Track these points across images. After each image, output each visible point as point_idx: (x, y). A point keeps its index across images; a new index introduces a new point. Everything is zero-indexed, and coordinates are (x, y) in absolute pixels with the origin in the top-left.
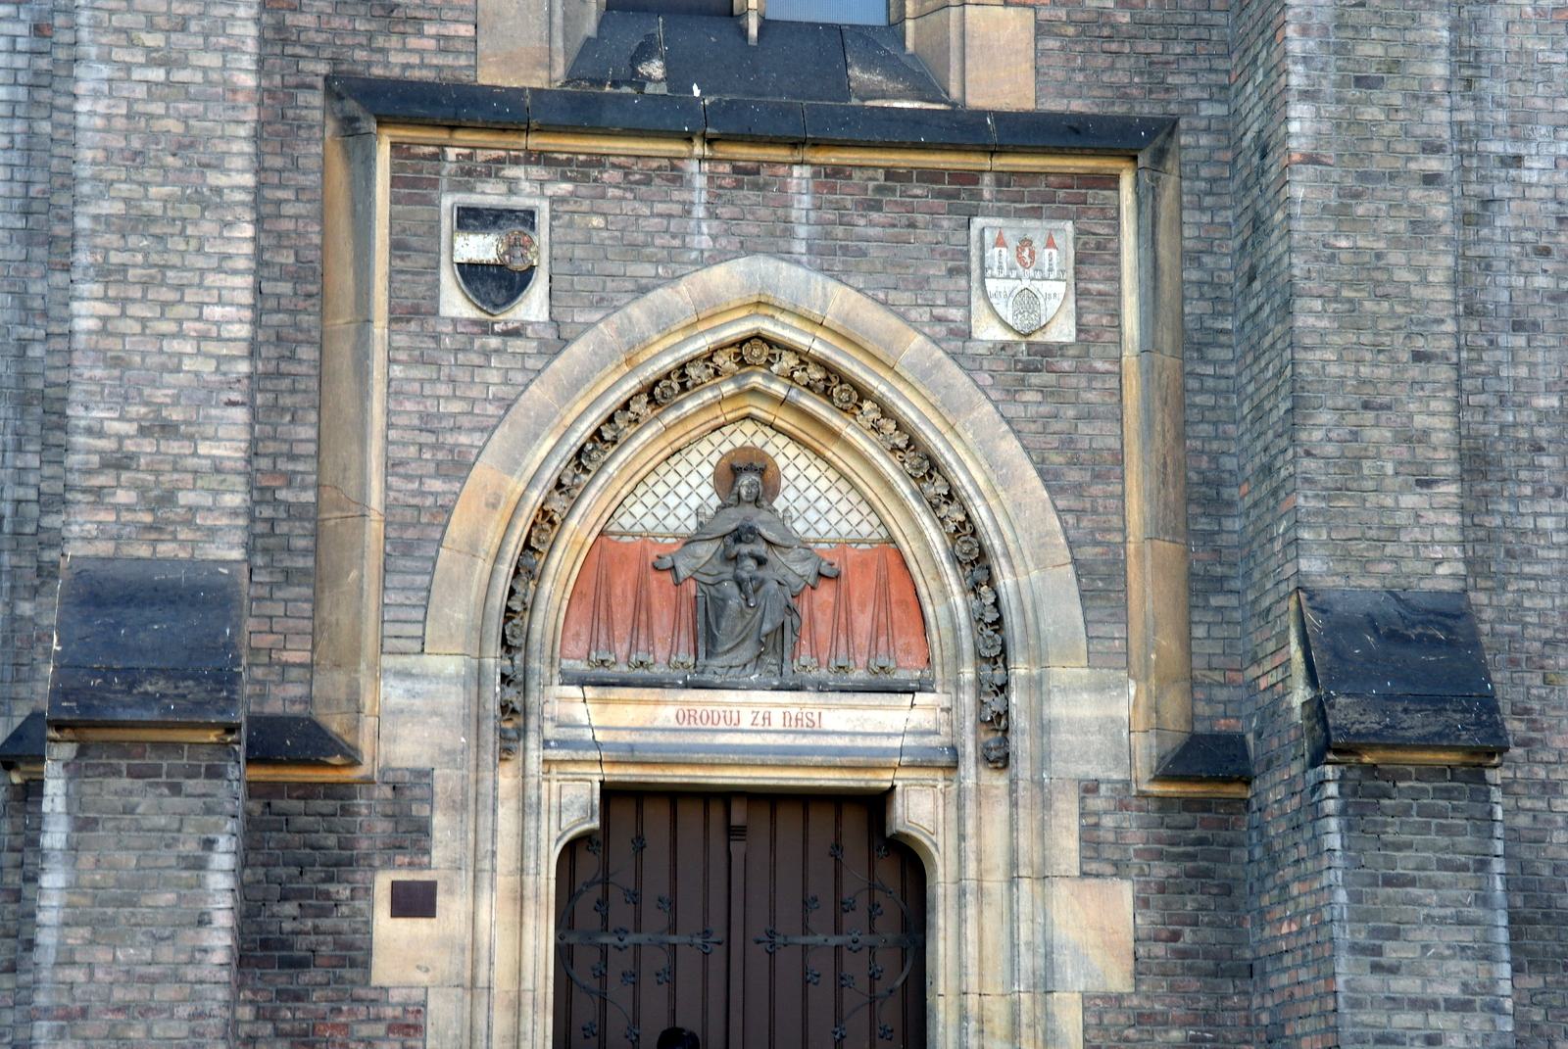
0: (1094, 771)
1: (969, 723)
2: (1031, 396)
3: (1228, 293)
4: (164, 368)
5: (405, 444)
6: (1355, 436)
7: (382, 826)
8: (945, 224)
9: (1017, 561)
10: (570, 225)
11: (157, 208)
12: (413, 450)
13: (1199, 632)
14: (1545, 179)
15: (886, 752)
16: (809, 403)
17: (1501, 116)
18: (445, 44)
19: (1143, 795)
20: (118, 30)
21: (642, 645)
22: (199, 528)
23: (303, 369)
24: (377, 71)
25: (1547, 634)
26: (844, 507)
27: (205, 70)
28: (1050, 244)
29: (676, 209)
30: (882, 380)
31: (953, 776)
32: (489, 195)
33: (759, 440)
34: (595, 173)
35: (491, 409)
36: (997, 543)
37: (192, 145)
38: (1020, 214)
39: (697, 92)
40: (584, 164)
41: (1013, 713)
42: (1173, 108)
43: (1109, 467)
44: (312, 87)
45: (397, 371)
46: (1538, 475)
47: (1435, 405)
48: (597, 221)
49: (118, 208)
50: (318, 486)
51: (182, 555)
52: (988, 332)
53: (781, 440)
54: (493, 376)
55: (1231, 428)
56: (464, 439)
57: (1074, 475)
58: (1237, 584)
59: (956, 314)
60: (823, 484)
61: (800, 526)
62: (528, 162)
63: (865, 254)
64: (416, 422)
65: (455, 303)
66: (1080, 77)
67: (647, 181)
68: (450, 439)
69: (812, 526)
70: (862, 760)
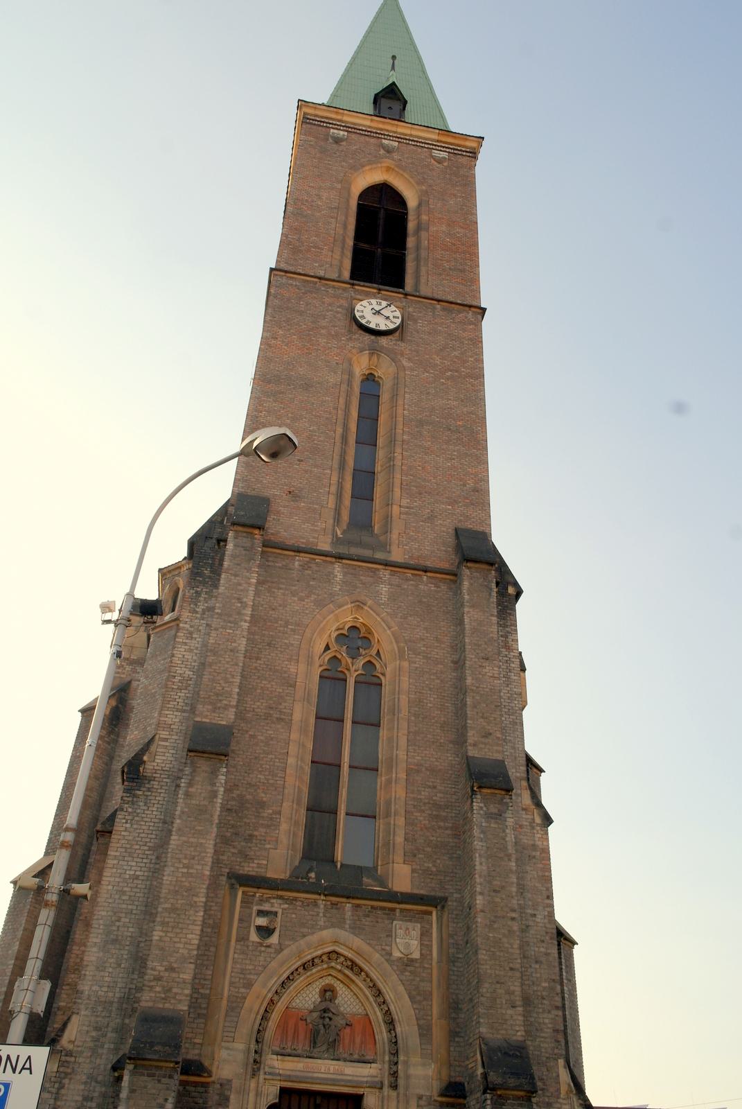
0: (421, 1092)
1: (387, 1074)
2: (407, 973)
3: (460, 947)
4: (174, 951)
5: (236, 977)
6: (495, 991)
7: (216, 1097)
8: (386, 922)
9: (402, 1023)
10: (287, 916)
11: (179, 906)
12: (237, 979)
13: (452, 1049)
14: (542, 921)
15: (362, 1082)
16: (347, 972)
17: (530, 903)
18: (259, 866)
19: (435, 1101)
20: (177, 858)
21: (295, 1043)
22: (177, 1000)
23: (211, 954)
24: (241, 872)
25: (547, 1055)
26: (354, 1004)
27: (197, 869)
28: (414, 930)
29: (315, 914)
30: (366, 965)
31: (381, 1091)
32: (266, 907)
33: (332, 982)
34: (294, 902)
35: (260, 969)
36: (396, 1018)
37: (191, 890)
38: (406, 921)
39: (323, 882)
40: (293, 900)
41: (399, 1072)
42: (447, 894)
43: (428, 996)
44: (224, 875)
45: (236, 956)
46: (543, 1006)
47: (516, 984)
48: (294, 916)
49: (169, 906)
50: (211, 988)
51: (172, 1007)
52: (397, 954)
53: (338, 982)
54: (262, 959)
55: (461, 987)
56: (252, 977)
57: (418, 998)
58: (462, 1035)
59: (388, 948)
60: (349, 996)
61: (342, 1009)
62: (277, 898)
63: (364, 929)
64: (239, 971)
65: (254, 937)
66: (423, 884)
67: (308, 905)
68: (248, 976)
69: (345, 1009)
70: (355, 1084)
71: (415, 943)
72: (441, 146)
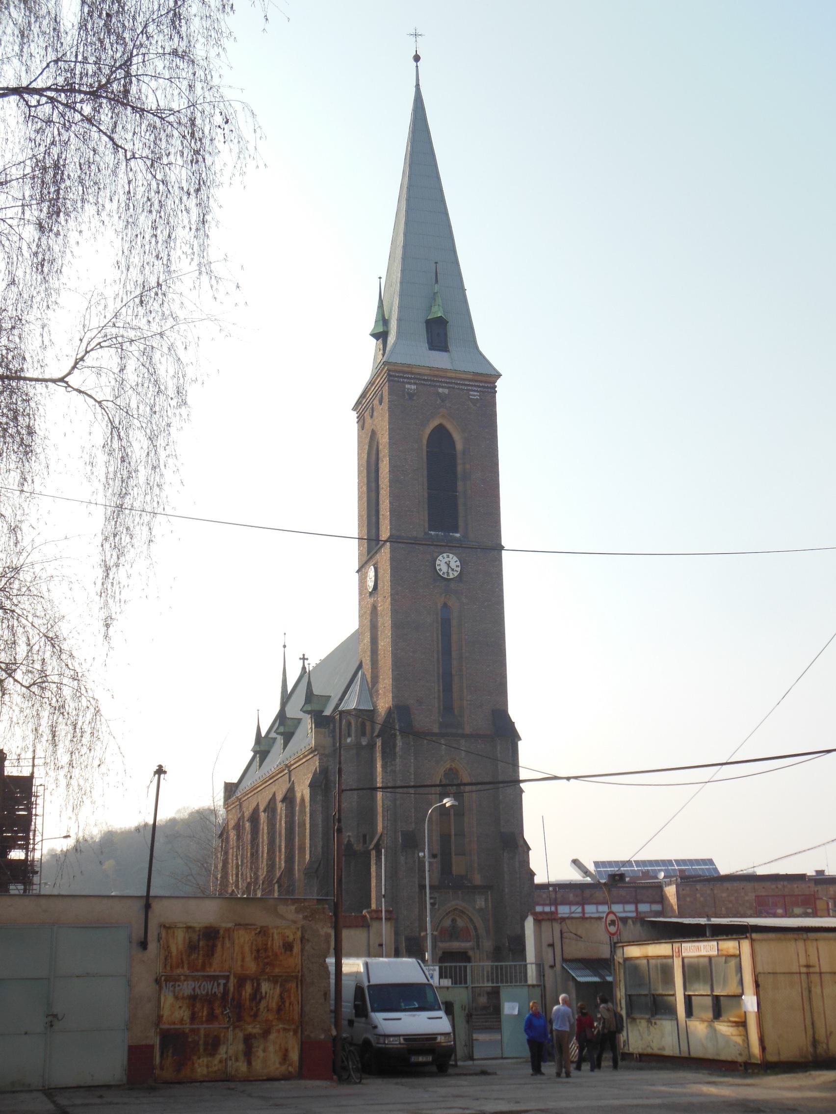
71: (483, 903)
72: (475, 386)
